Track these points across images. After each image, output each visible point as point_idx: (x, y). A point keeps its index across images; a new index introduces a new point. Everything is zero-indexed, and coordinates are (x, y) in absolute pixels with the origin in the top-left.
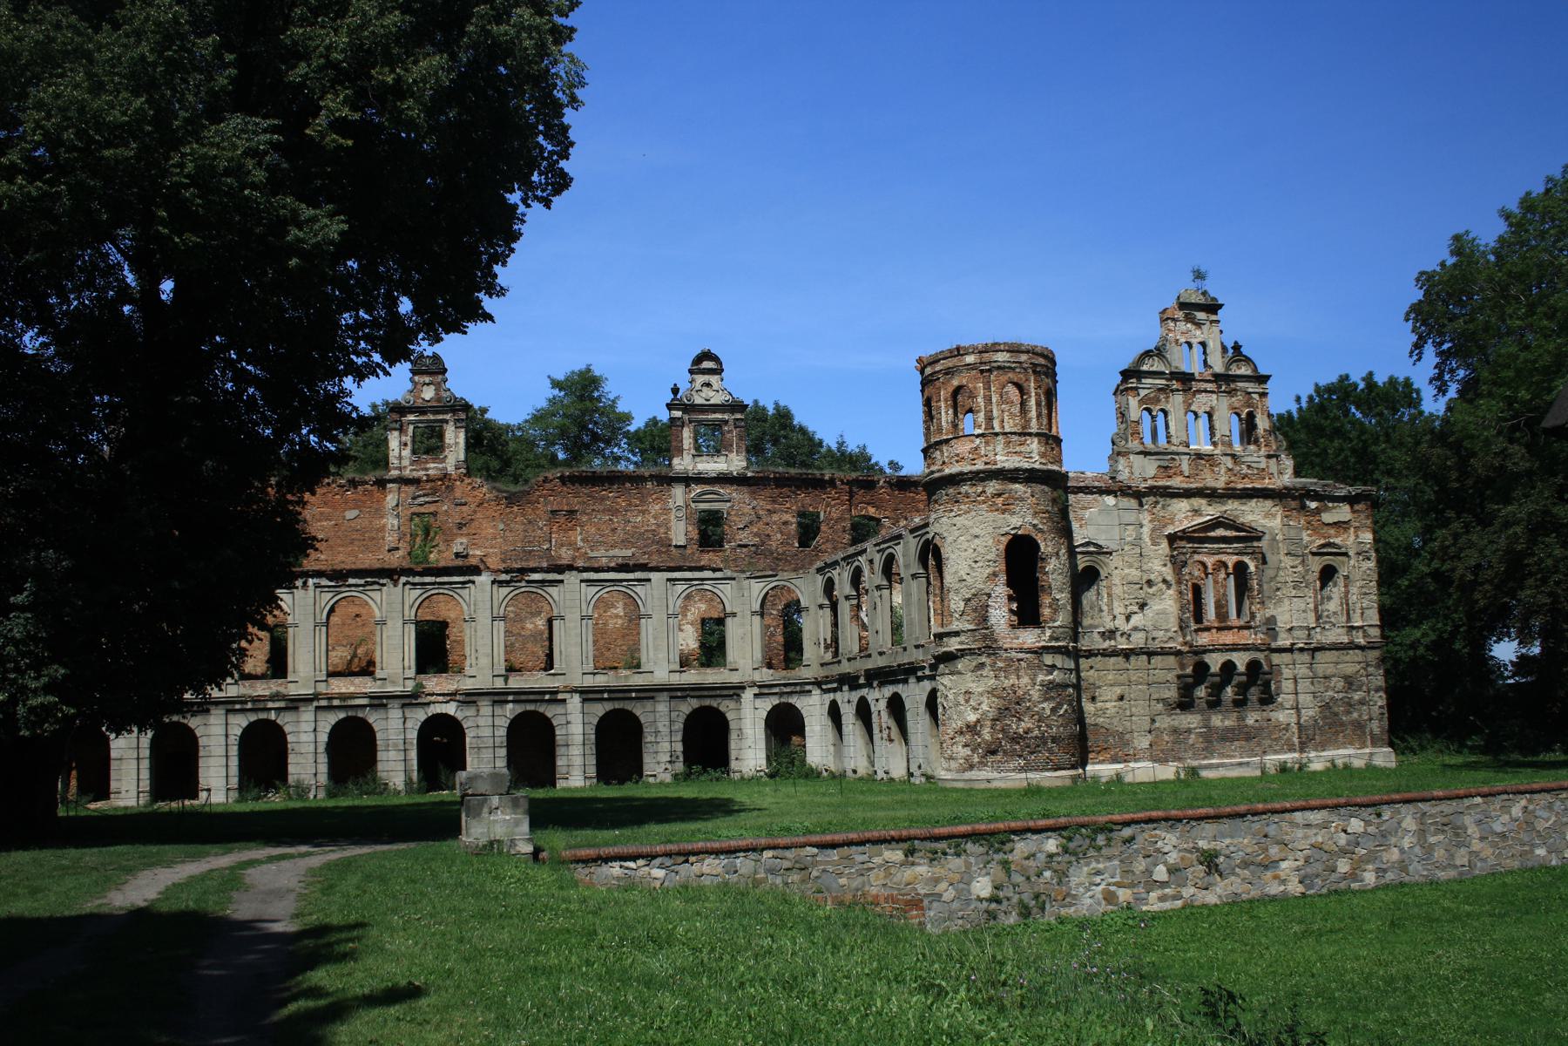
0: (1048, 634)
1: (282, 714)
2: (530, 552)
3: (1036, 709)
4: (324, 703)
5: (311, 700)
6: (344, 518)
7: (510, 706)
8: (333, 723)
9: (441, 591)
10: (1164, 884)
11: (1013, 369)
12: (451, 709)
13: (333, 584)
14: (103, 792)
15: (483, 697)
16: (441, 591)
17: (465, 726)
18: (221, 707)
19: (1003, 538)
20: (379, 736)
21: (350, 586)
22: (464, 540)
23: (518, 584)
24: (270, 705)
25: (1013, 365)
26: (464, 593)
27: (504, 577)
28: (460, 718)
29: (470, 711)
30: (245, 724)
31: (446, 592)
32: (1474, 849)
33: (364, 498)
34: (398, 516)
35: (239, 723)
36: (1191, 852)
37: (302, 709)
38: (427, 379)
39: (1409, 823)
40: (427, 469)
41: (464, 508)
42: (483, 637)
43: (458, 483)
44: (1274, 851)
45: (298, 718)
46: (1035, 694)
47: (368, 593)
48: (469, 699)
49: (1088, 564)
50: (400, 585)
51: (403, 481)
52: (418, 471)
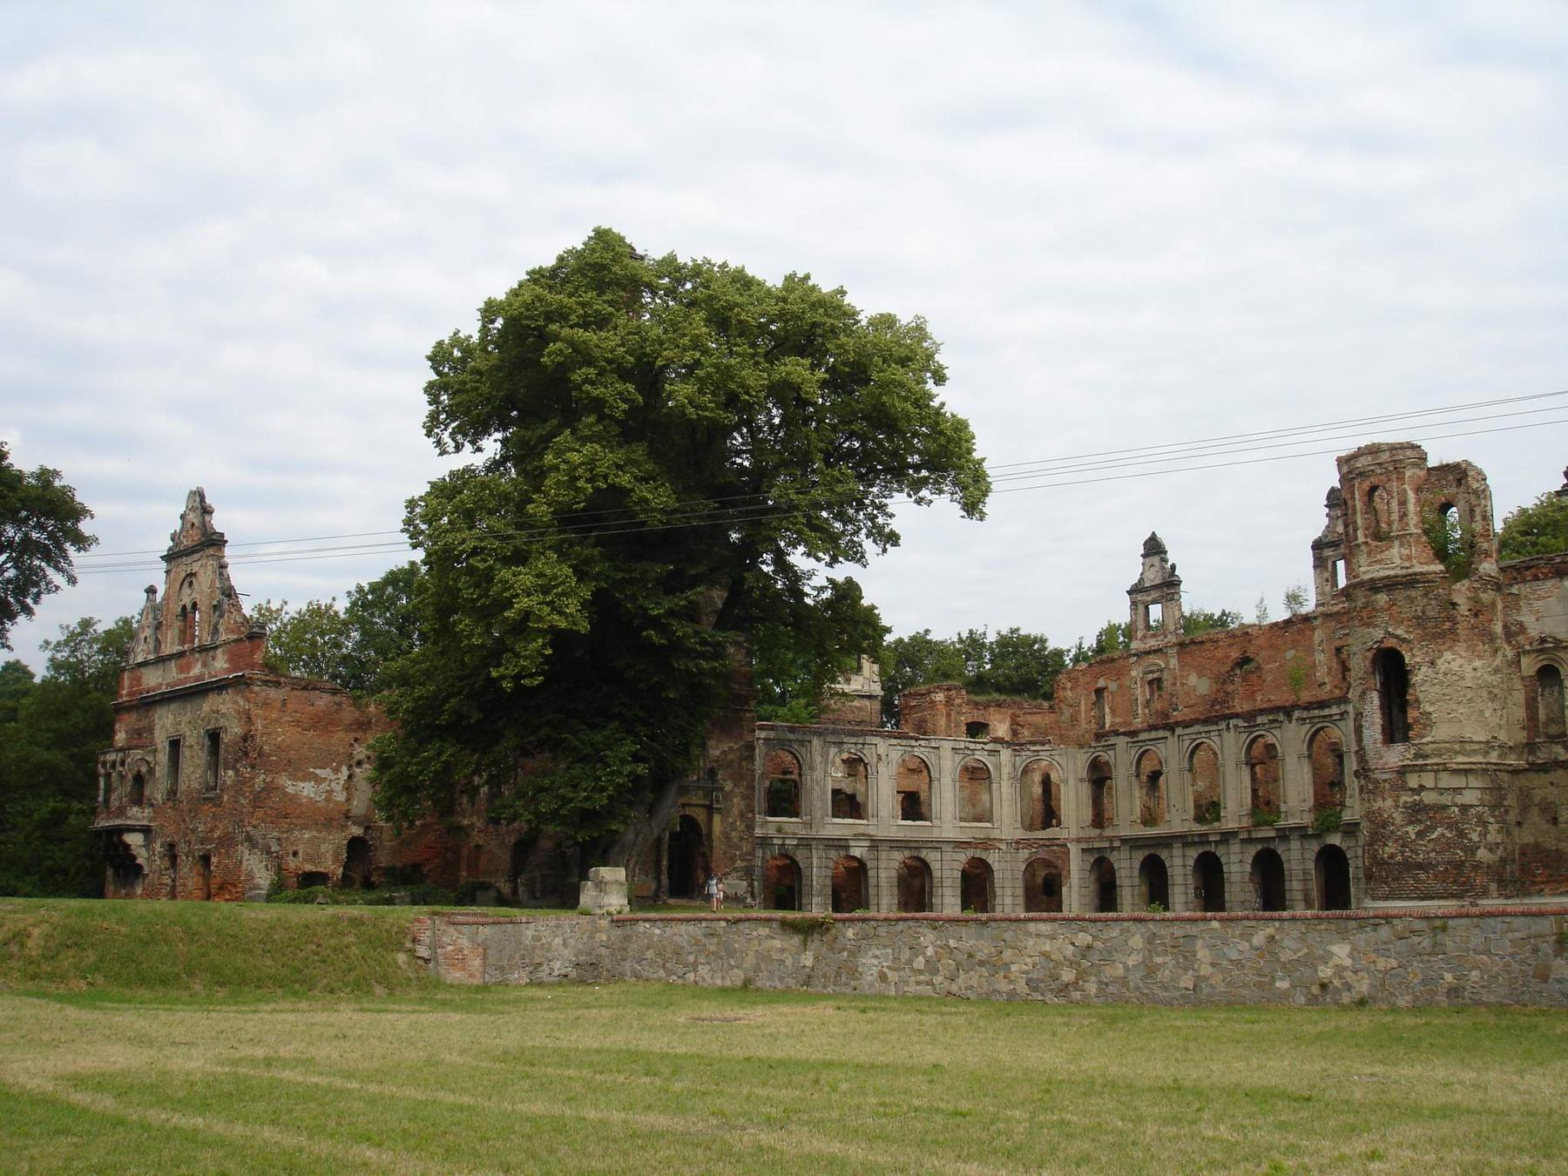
0: (1413, 752)
3: (1399, 833)
4: (1245, 836)
9: (1325, 724)
10: (920, 972)
11: (1373, 471)
16: (1325, 724)
17: (1348, 857)
19: (1368, 654)
20: (1286, 866)
21: (1258, 725)
25: (1372, 468)
28: (1344, 849)
30: (1195, 856)
32: (1202, 973)
36: (942, 948)
37: (1231, 842)
39: (1137, 941)
44: (1007, 955)
45: (1229, 849)
46: (1398, 817)
49: (1545, 663)
50: (1294, 721)
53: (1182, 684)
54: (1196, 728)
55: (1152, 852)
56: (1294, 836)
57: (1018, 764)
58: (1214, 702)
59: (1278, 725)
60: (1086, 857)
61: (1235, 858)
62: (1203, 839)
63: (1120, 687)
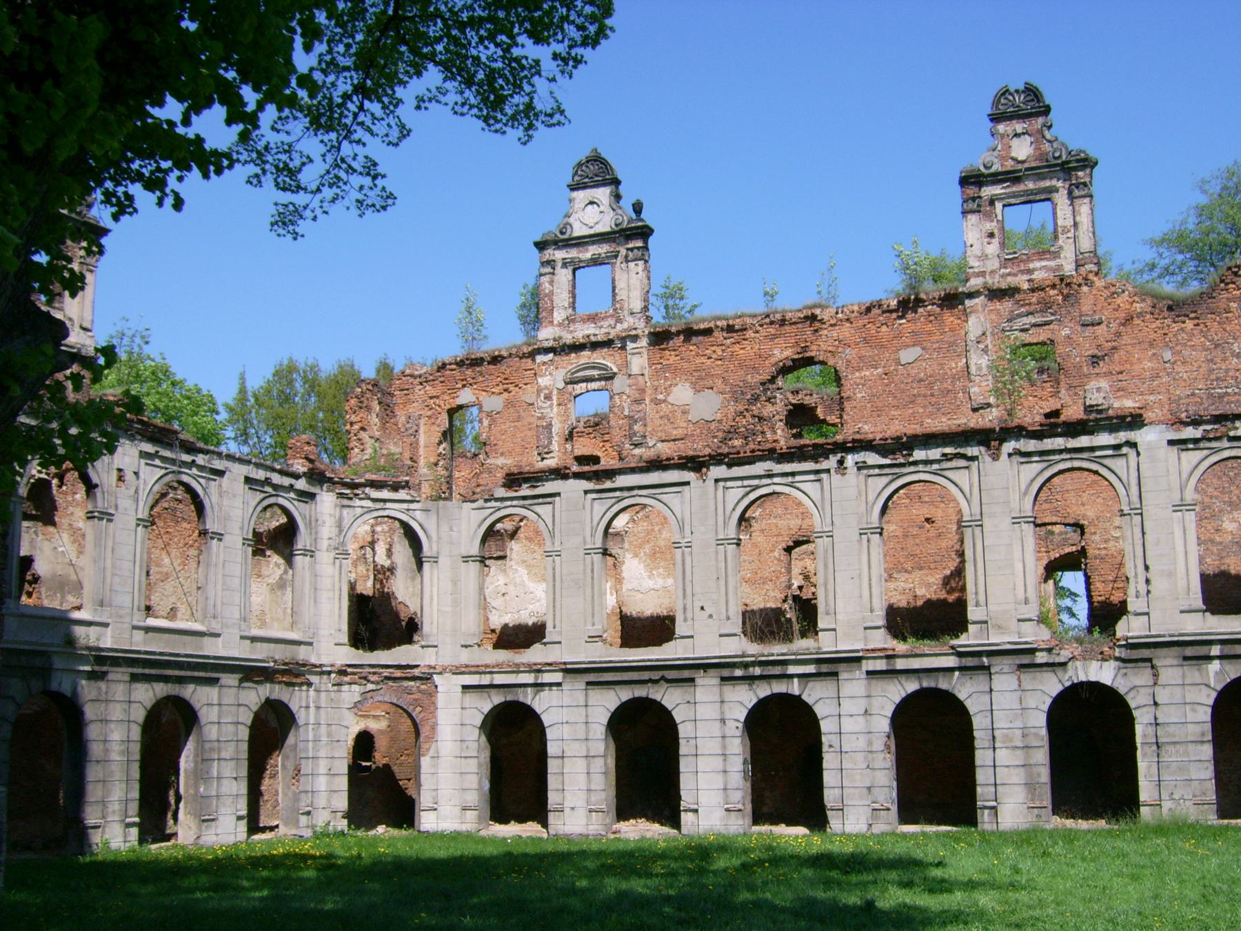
1: (810, 685)
2: (1221, 396)
4: (881, 665)
5: (858, 660)
6: (898, 362)
7: (1215, 666)
8: (897, 700)
12: (1104, 673)
13: (887, 461)
14: (537, 809)
15: (1165, 651)
16: (1077, 464)
17: (1132, 704)
18: (712, 672)
21: (915, 463)
22: (1104, 384)
23: (1214, 444)
24: (792, 670)
26: (1118, 464)
27: (1190, 432)
28: (1122, 691)
29: (1141, 677)
31: (1085, 465)
33: (929, 327)
34: (985, 350)
35: (743, 699)
37: (843, 676)
38: (1019, 127)
40: (1030, 272)
41: (1100, 330)
42: (1158, 542)
43: (1085, 289)
47: (947, 473)
48: (1136, 654)
50: (1004, 457)
51: (996, 294)
52: (1015, 275)
53: (657, 402)
54: (760, 468)
55: (640, 692)
56: (1002, 666)
57: (346, 523)
58: (731, 432)
59: (962, 463)
60: (471, 699)
61: (848, 706)
62: (774, 669)
63: (509, 404)
